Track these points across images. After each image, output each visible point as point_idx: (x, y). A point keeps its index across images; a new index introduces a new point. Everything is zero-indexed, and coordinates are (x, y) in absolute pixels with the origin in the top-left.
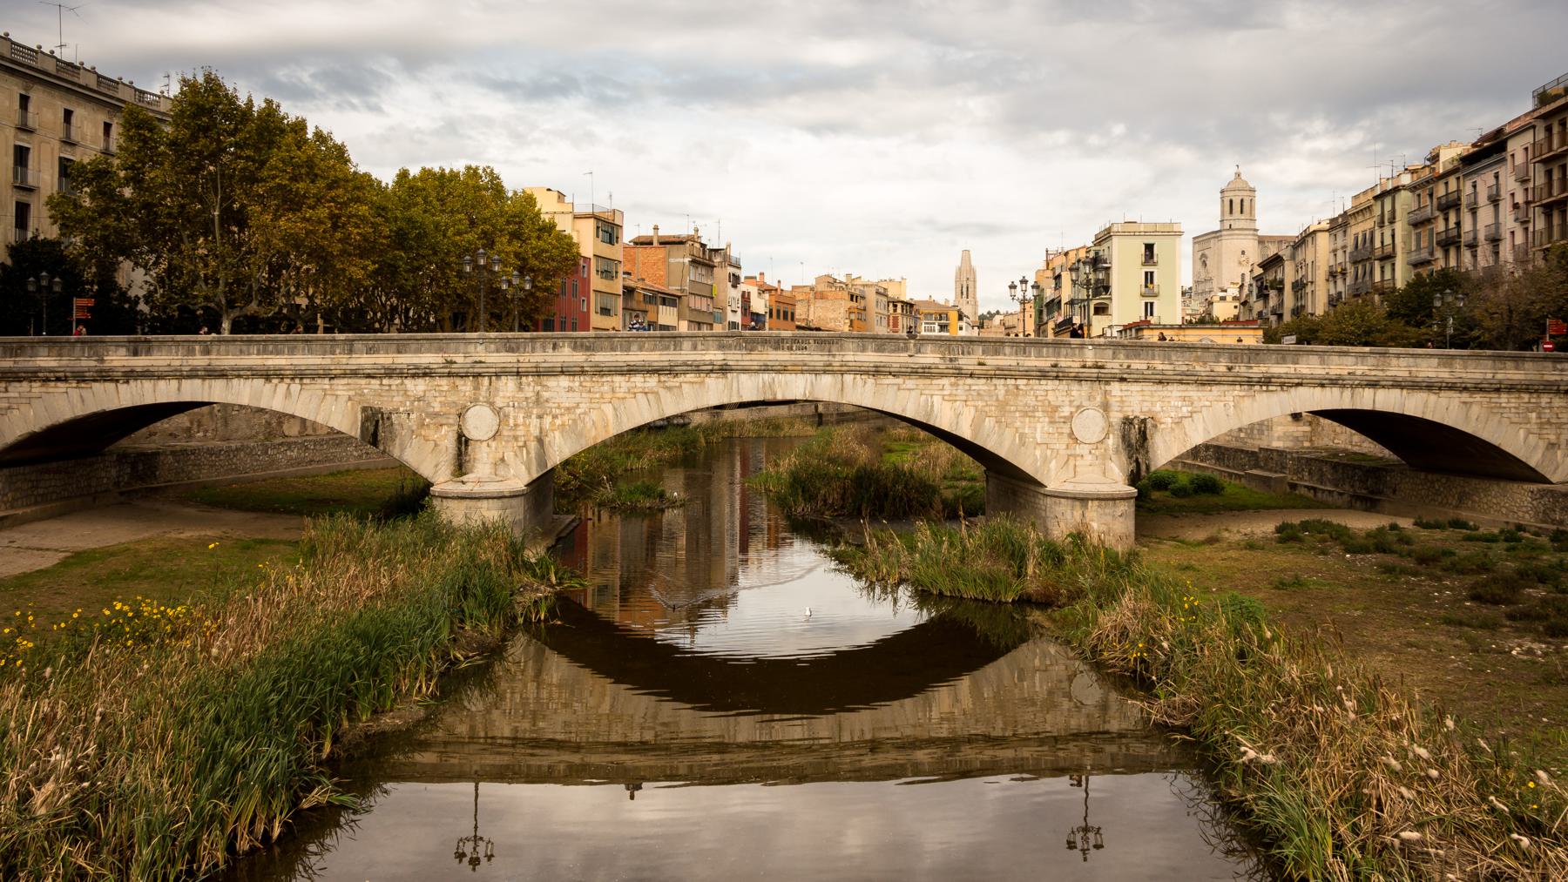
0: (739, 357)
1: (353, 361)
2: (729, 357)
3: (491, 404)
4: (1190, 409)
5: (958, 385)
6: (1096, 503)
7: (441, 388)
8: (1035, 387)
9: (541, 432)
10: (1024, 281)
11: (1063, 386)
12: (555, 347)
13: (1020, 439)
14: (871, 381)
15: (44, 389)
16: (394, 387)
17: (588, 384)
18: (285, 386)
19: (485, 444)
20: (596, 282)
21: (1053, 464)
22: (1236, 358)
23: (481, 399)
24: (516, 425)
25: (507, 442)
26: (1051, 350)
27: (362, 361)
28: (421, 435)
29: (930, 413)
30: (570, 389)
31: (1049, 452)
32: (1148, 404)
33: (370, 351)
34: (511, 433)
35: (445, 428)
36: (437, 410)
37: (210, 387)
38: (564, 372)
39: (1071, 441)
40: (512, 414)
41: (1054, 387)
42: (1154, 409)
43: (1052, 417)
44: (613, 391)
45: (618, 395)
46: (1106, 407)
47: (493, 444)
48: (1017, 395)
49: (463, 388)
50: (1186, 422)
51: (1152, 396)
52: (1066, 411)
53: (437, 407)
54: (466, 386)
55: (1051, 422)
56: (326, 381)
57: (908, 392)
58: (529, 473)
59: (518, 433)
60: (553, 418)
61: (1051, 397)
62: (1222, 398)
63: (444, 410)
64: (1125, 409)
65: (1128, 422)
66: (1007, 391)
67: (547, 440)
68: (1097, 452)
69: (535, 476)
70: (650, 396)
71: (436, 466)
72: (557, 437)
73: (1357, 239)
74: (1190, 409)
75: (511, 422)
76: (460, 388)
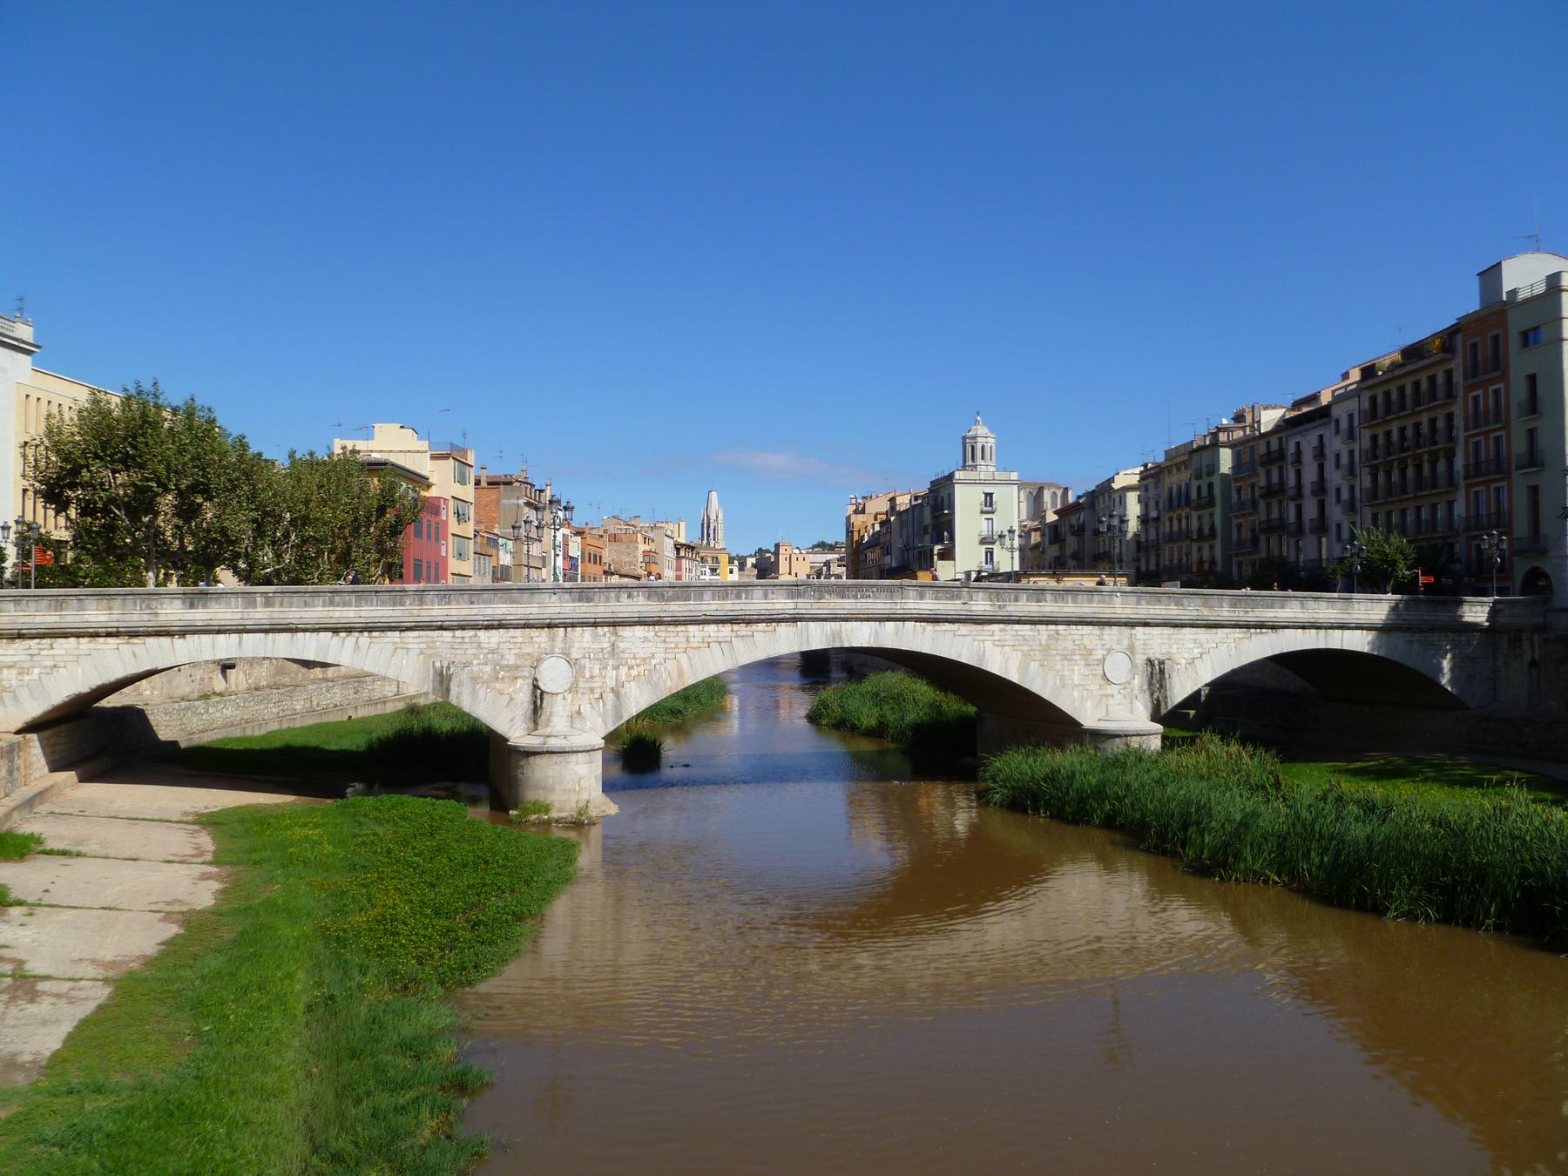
0: (808, 606)
1: (423, 613)
4: (1200, 650)
7: (515, 640)
8: (1073, 632)
10: (1011, 531)
12: (629, 596)
13: (1061, 681)
15: (92, 646)
16: (467, 640)
17: (663, 634)
18: (354, 639)
19: (560, 696)
20: (453, 526)
21: (1089, 704)
22: (1235, 604)
23: (557, 650)
24: (592, 677)
25: (583, 694)
27: (434, 613)
28: (495, 688)
29: (982, 658)
30: (645, 639)
32: (1167, 646)
34: (587, 685)
35: (520, 681)
36: (512, 662)
37: (274, 641)
38: (642, 622)
40: (588, 665)
41: (1089, 632)
42: (1171, 651)
43: (1087, 660)
44: (688, 641)
45: (691, 645)
47: (569, 697)
48: (1057, 640)
49: (538, 640)
50: (1197, 662)
51: (1170, 639)
52: (1099, 654)
53: (511, 659)
54: (541, 637)
55: (1086, 665)
56: (397, 633)
57: (962, 638)
59: (594, 685)
60: (629, 669)
61: (1086, 641)
62: (1225, 640)
63: (519, 662)
64: (1148, 651)
65: (1150, 662)
66: (1049, 636)
67: (623, 691)
69: (611, 728)
71: (512, 720)
72: (633, 688)
73: (1171, 490)
74: (1200, 650)
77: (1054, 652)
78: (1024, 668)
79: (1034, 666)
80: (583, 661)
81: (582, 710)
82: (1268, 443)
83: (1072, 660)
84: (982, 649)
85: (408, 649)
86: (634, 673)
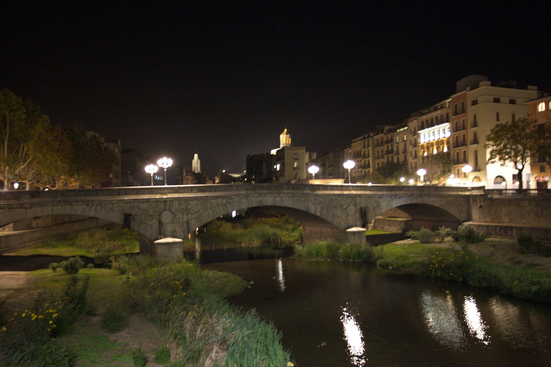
2: (249, 192)
3: (170, 211)
16: (135, 206)
30: (197, 205)
31: (341, 219)
46: (355, 205)
47: (172, 225)
52: (345, 206)
53: (151, 213)
73: (355, 152)
75: (178, 217)
78: (321, 212)
79: (325, 211)
80: (176, 212)
82: (388, 137)
85: (115, 210)
86: (193, 216)
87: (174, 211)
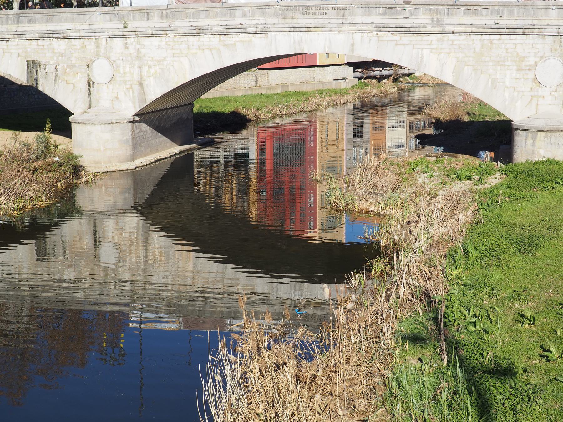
2: (269, 22)
3: (108, 58)
5: (443, 40)
6: (543, 134)
7: (76, 47)
9: (141, 78)
11: (530, 39)
14: (374, 37)
16: (46, 47)
19: (105, 86)
24: (124, 73)
26: (521, 10)
30: (159, 47)
33: (30, 22)
35: (79, 75)
36: (74, 62)
39: (535, 85)
47: (111, 87)
54: (90, 45)
55: (518, 70)
58: (135, 107)
60: (149, 67)
67: (145, 83)
68: (557, 94)
70: (214, 51)
76: (87, 47)
77: (487, 59)
81: (119, 96)
83: (505, 66)
84: (420, 56)
85: (11, 53)
86: (152, 71)
87: (114, 59)
